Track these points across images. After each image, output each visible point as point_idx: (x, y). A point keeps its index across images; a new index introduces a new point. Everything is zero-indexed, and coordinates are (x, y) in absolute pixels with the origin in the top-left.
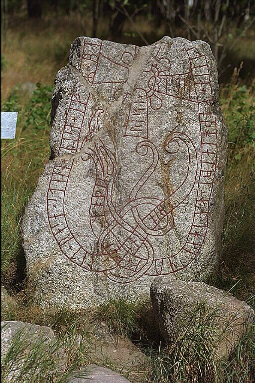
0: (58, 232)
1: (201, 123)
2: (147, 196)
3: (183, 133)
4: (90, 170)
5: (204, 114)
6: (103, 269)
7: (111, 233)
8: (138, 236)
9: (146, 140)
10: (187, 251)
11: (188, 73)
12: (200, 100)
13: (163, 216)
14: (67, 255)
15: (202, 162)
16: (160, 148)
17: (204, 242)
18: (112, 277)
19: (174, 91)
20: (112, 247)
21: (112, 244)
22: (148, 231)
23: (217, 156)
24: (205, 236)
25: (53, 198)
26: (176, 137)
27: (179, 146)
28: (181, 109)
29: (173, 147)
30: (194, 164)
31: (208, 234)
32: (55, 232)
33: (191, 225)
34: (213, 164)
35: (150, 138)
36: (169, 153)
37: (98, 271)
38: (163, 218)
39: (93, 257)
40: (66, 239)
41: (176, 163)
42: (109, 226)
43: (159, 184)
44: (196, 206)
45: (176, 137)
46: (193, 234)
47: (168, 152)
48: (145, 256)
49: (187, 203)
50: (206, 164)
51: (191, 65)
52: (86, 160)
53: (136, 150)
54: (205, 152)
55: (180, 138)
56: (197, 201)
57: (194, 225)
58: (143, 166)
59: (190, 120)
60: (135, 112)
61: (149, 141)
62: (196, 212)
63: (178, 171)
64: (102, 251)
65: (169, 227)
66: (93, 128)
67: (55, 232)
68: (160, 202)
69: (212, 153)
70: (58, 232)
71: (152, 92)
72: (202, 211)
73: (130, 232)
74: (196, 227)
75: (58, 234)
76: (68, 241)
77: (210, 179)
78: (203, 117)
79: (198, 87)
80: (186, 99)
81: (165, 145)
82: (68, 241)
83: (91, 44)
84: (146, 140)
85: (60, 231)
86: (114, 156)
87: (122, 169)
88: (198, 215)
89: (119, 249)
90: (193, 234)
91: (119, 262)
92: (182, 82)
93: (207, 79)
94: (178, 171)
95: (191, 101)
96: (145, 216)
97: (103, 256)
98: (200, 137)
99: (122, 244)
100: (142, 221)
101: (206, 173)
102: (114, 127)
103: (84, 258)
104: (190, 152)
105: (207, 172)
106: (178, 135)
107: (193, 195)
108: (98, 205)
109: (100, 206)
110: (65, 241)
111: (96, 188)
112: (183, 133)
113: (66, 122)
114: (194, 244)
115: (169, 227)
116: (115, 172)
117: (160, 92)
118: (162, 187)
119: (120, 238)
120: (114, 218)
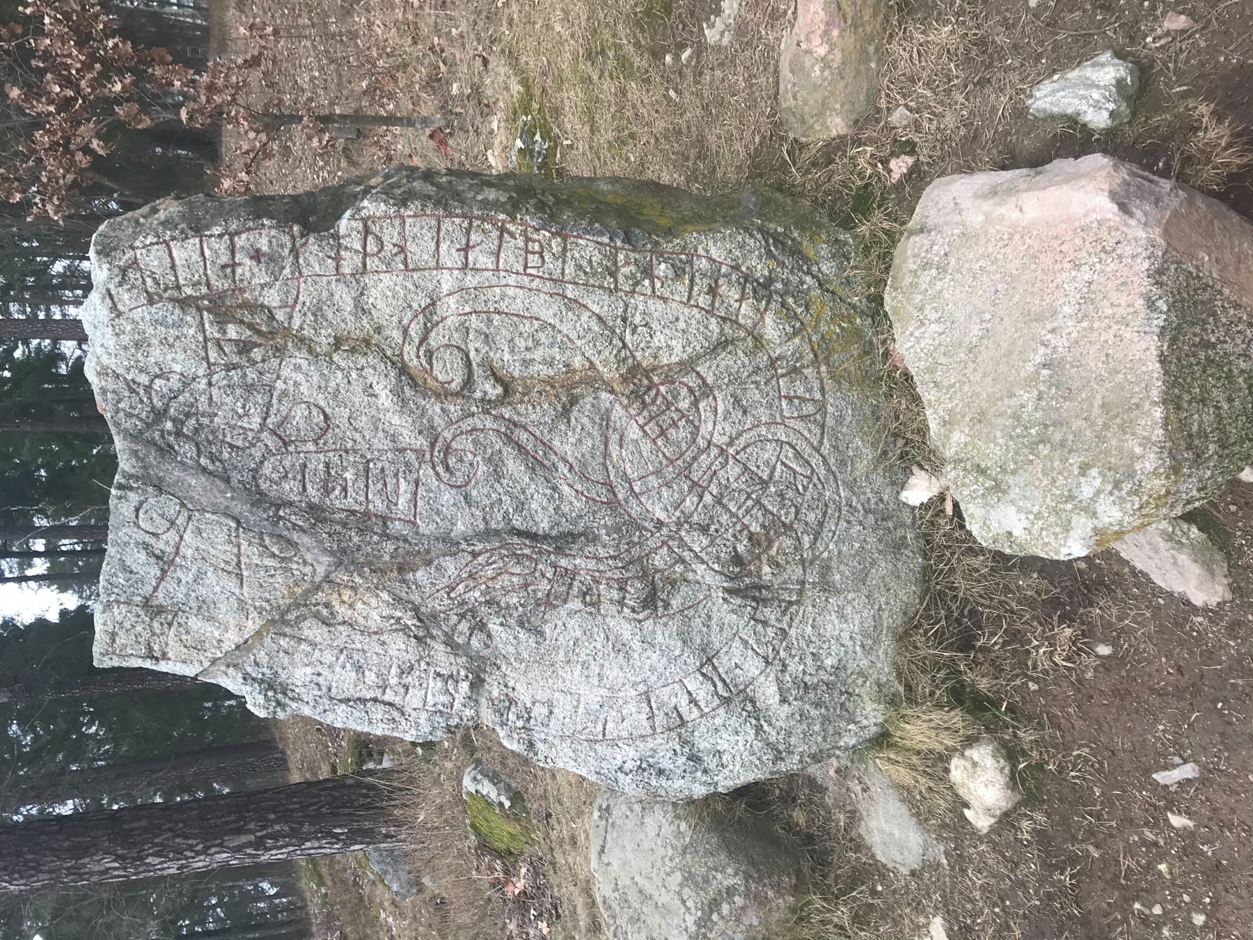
0: (696, 705)
3: (405, 332)
5: (337, 259)
6: (799, 570)
9: (428, 456)
11: (199, 309)
12: (292, 273)
14: (757, 672)
16: (454, 409)
19: (263, 361)
20: (741, 548)
21: (735, 548)
22: (702, 443)
23: (478, 218)
24: (721, 263)
25: (600, 727)
26: (418, 357)
28: (324, 340)
29: (448, 371)
30: (503, 298)
33: (686, 311)
34: (503, 230)
36: (469, 378)
37: (803, 583)
38: (664, 398)
40: (716, 679)
41: (505, 358)
42: (682, 560)
43: (565, 413)
45: (418, 357)
46: (713, 302)
47: (469, 382)
48: (769, 452)
49: (624, 320)
50: (502, 255)
51: (171, 299)
52: (489, 636)
53: (460, 487)
54: (466, 259)
55: (421, 343)
57: (689, 298)
58: (513, 465)
59: (361, 309)
60: (337, 492)
61: (432, 445)
62: (649, 292)
63: (527, 349)
64: (750, 574)
65: (691, 380)
66: (393, 621)
67: (696, 713)
68: (617, 406)
70: (696, 705)
71: (271, 441)
72: (648, 272)
74: (694, 293)
75: (702, 704)
79: (248, 275)
80: (291, 317)
81: (443, 394)
83: (113, 635)
84: (428, 456)
85: (693, 701)
86: (480, 554)
88: (658, 285)
90: (713, 302)
91: (784, 524)
92: (232, 331)
93: (222, 246)
94: (527, 349)
95: (296, 302)
101: (530, 257)
102: (387, 558)
104: (467, 309)
105: (527, 252)
107: (598, 303)
108: (624, 598)
110: (720, 685)
111: (575, 604)
112: (405, 332)
115: (691, 380)
116: (527, 551)
117: (268, 409)
118: (574, 400)
119: (717, 526)
120: (661, 547)
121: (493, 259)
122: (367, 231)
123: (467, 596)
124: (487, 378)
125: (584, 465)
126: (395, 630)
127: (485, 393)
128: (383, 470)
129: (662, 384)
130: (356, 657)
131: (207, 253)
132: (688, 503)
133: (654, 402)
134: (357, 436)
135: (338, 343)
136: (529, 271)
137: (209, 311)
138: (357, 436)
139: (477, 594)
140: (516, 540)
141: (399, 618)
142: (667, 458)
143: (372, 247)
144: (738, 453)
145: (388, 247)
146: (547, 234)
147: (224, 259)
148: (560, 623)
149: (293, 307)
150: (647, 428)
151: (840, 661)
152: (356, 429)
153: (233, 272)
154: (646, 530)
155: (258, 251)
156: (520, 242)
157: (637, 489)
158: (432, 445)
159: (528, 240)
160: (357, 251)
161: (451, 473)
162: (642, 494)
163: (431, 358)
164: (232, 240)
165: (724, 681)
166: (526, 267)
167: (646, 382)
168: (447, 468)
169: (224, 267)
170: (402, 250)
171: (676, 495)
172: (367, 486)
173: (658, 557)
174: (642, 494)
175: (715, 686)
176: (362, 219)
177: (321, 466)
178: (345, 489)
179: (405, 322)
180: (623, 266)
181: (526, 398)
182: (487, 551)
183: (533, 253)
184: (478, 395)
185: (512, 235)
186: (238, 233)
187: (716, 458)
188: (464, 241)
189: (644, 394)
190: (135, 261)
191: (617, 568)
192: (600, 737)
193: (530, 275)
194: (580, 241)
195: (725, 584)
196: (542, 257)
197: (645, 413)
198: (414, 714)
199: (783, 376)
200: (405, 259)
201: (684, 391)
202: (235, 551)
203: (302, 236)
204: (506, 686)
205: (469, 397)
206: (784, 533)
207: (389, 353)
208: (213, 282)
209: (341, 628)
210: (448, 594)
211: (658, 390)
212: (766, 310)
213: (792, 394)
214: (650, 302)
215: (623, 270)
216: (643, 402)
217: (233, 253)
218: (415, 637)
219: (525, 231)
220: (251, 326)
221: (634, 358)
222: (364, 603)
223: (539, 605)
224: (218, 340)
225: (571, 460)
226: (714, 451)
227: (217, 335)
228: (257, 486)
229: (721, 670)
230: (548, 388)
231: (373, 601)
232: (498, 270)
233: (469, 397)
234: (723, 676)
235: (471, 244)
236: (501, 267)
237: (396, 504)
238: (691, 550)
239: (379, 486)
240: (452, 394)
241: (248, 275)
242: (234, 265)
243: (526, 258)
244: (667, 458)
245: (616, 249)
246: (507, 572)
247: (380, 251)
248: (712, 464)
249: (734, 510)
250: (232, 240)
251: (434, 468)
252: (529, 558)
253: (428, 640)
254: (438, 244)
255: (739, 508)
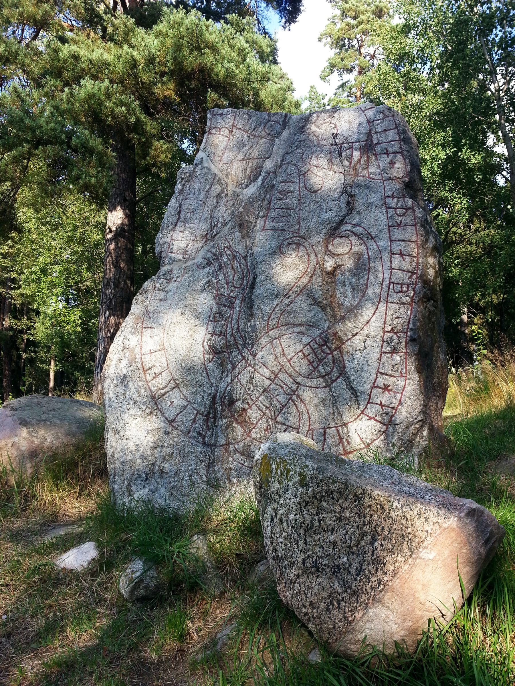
1: (389, 210)
2: (297, 322)
3: (358, 225)
4: (208, 282)
5: (393, 197)
7: (236, 380)
8: (282, 387)
9: (295, 235)
10: (370, 418)
11: (366, 141)
13: (324, 355)
14: (166, 415)
15: (392, 269)
17: (400, 403)
18: (237, 456)
21: (239, 400)
22: (299, 379)
24: (402, 393)
26: (346, 231)
27: (351, 244)
31: (408, 388)
32: (149, 378)
33: (374, 371)
34: (413, 273)
35: (303, 232)
38: (325, 358)
39: (207, 421)
40: (166, 390)
44: (383, 341)
45: (346, 231)
50: (399, 271)
52: (204, 268)
53: (280, 249)
54: (396, 254)
55: (352, 232)
56: (384, 332)
57: (381, 373)
59: (368, 206)
61: (301, 237)
62: (384, 350)
65: (335, 373)
69: (408, 256)
70: (154, 378)
73: (269, 379)
75: (154, 381)
76: (168, 392)
77: (406, 296)
78: (393, 203)
79: (383, 159)
82: (168, 392)
84: (295, 235)
86: (245, 260)
87: (257, 280)
89: (250, 407)
91: (250, 431)
93: (397, 148)
96: (293, 354)
97: (225, 421)
98: (387, 230)
99: (255, 399)
100: (289, 361)
101: (400, 286)
102: (247, 218)
103: (194, 421)
104: (370, 253)
106: (349, 227)
108: (216, 335)
109: (220, 336)
110: (162, 391)
112: (358, 225)
113: (179, 218)
114: (381, 404)
118: (324, 309)
120: (242, 356)
121: (397, 267)
122: (407, 209)
123: (225, 255)
124: (336, 263)
125: (289, 313)
126: (211, 225)
127: (327, 262)
128: (290, 215)
129: (333, 356)
130: (201, 208)
131: (393, 143)
132: (265, 370)
133: (322, 351)
134: (307, 204)
135: (352, 196)
136: (392, 285)
137: (365, 145)
138: (307, 204)
139: (225, 260)
140: (251, 277)
141: (217, 226)
142: (291, 359)
143: (399, 211)
144: (293, 401)
145: (400, 219)
146: (412, 294)
147: (390, 150)
148: (206, 301)
149: (369, 177)
150: (308, 346)
151: (167, 473)
152: (310, 203)
153: (384, 153)
154: (252, 347)
155: (395, 163)
156: (407, 281)
157: (274, 342)
158: (301, 237)
159: (408, 285)
160: (397, 205)
161: (287, 246)
162: (272, 345)
163: (345, 236)
164: (399, 152)
165: (164, 395)
166: (394, 283)
167: (334, 347)
168: (290, 244)
169: (386, 149)
170: (399, 225)
171: (270, 363)
172: (282, 209)
173: (236, 354)
174: (272, 345)
175: (162, 389)
176: (413, 207)
177: (292, 189)
178: (281, 199)
179: (363, 225)
180: (397, 336)
181: (325, 283)
182: (246, 263)
183: (401, 287)
184: (327, 258)
185: (410, 277)
186: (402, 155)
187: (290, 388)
188: (405, 253)
189: (327, 346)
190: (387, 117)
191: (232, 330)
192: (144, 326)
193: (390, 285)
194: (409, 312)
195: (218, 394)
196: (399, 292)
197: (316, 346)
198: (170, 235)
199: (338, 431)
200: (394, 226)
201: (328, 369)
202: (255, 157)
203: (404, 182)
204: (178, 277)
205: (325, 254)
206: (245, 432)
207: (347, 218)
208: (379, 146)
209: (215, 201)
210: (227, 247)
211: (330, 354)
212: (376, 420)
213: (327, 436)
214: (378, 350)
215: (395, 336)
216: (323, 345)
217: (393, 153)
218: (207, 234)
219: (413, 284)
220: (359, 160)
221: (347, 341)
222: (226, 210)
223: (216, 291)
224: (352, 147)
225: (292, 305)
226: (294, 387)
227: (354, 147)
228: (284, 164)
229: (171, 392)
230: (330, 293)
231: (227, 214)
232: (392, 269)
233: (325, 254)
234: (167, 395)
235: (404, 257)
236: (393, 270)
237: (273, 221)
238: (239, 374)
239: (282, 214)
240: (327, 246)
241: (383, 159)
242: (387, 154)
243: (398, 284)
244: (291, 359)
245: (406, 333)
246: (235, 273)
247: (397, 215)
248: (287, 385)
249: (260, 399)
250: (399, 152)
251: (291, 238)
252: (242, 284)
253: (204, 240)
254: (404, 241)
255: (261, 403)
